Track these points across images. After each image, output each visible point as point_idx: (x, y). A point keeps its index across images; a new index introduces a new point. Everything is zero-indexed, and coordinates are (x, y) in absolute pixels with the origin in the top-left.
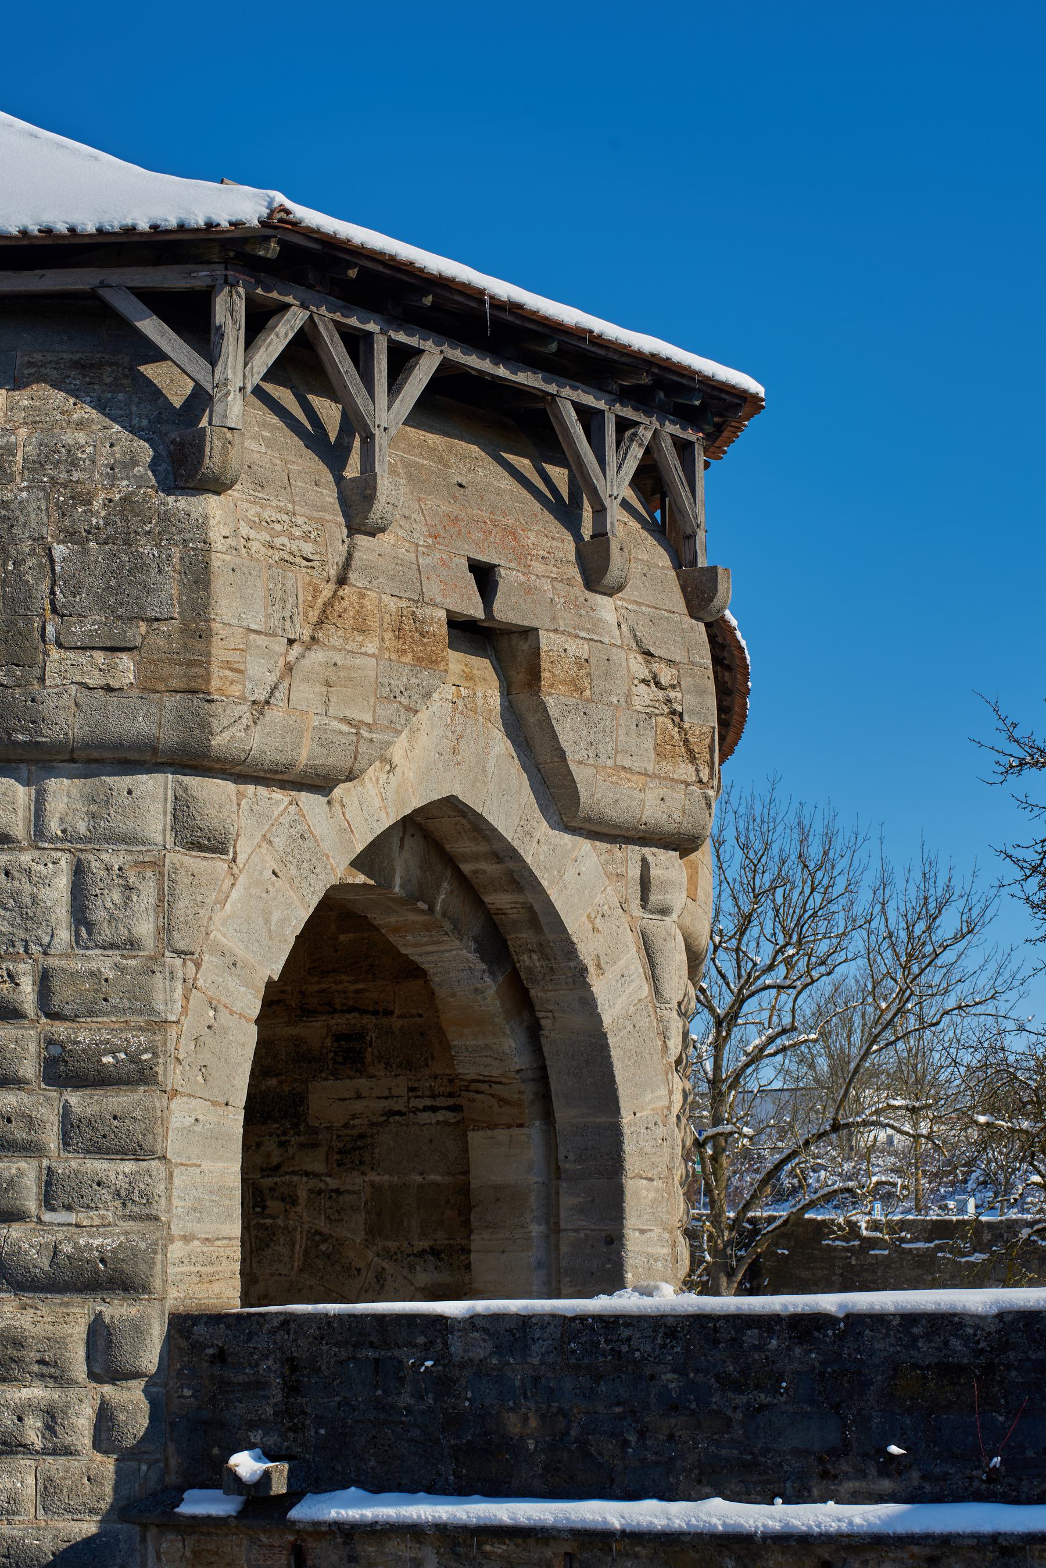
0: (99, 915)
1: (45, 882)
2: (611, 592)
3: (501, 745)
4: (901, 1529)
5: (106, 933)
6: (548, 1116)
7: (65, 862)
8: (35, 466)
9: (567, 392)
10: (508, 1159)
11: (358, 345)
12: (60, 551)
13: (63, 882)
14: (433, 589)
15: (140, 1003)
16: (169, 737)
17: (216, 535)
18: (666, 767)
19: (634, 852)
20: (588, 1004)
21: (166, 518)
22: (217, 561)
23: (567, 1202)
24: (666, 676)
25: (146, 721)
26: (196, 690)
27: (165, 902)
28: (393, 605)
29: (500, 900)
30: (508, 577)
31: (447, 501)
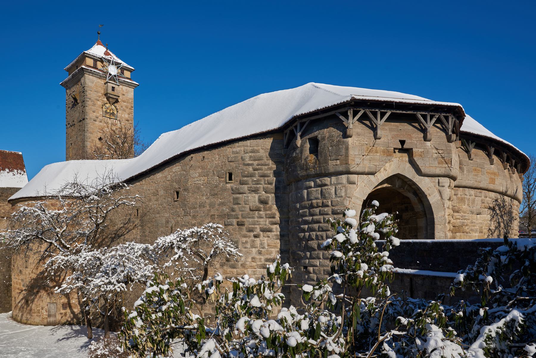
0: (337, 193)
1: (331, 190)
2: (430, 141)
3: (408, 165)
4: (418, 274)
5: (338, 195)
6: (426, 217)
7: (334, 187)
8: (328, 138)
9: (419, 113)
10: (421, 223)
11: (375, 114)
12: (330, 148)
13: (334, 189)
14: (391, 145)
15: (342, 203)
16: (344, 170)
17: (350, 143)
18: (440, 165)
19: (437, 179)
20: (428, 200)
21: (343, 142)
22: (349, 147)
23: (428, 228)
24: (441, 152)
25: (341, 169)
26: (347, 163)
27: (346, 191)
28: (383, 148)
29: (414, 187)
30: (408, 141)
31: (389, 132)
